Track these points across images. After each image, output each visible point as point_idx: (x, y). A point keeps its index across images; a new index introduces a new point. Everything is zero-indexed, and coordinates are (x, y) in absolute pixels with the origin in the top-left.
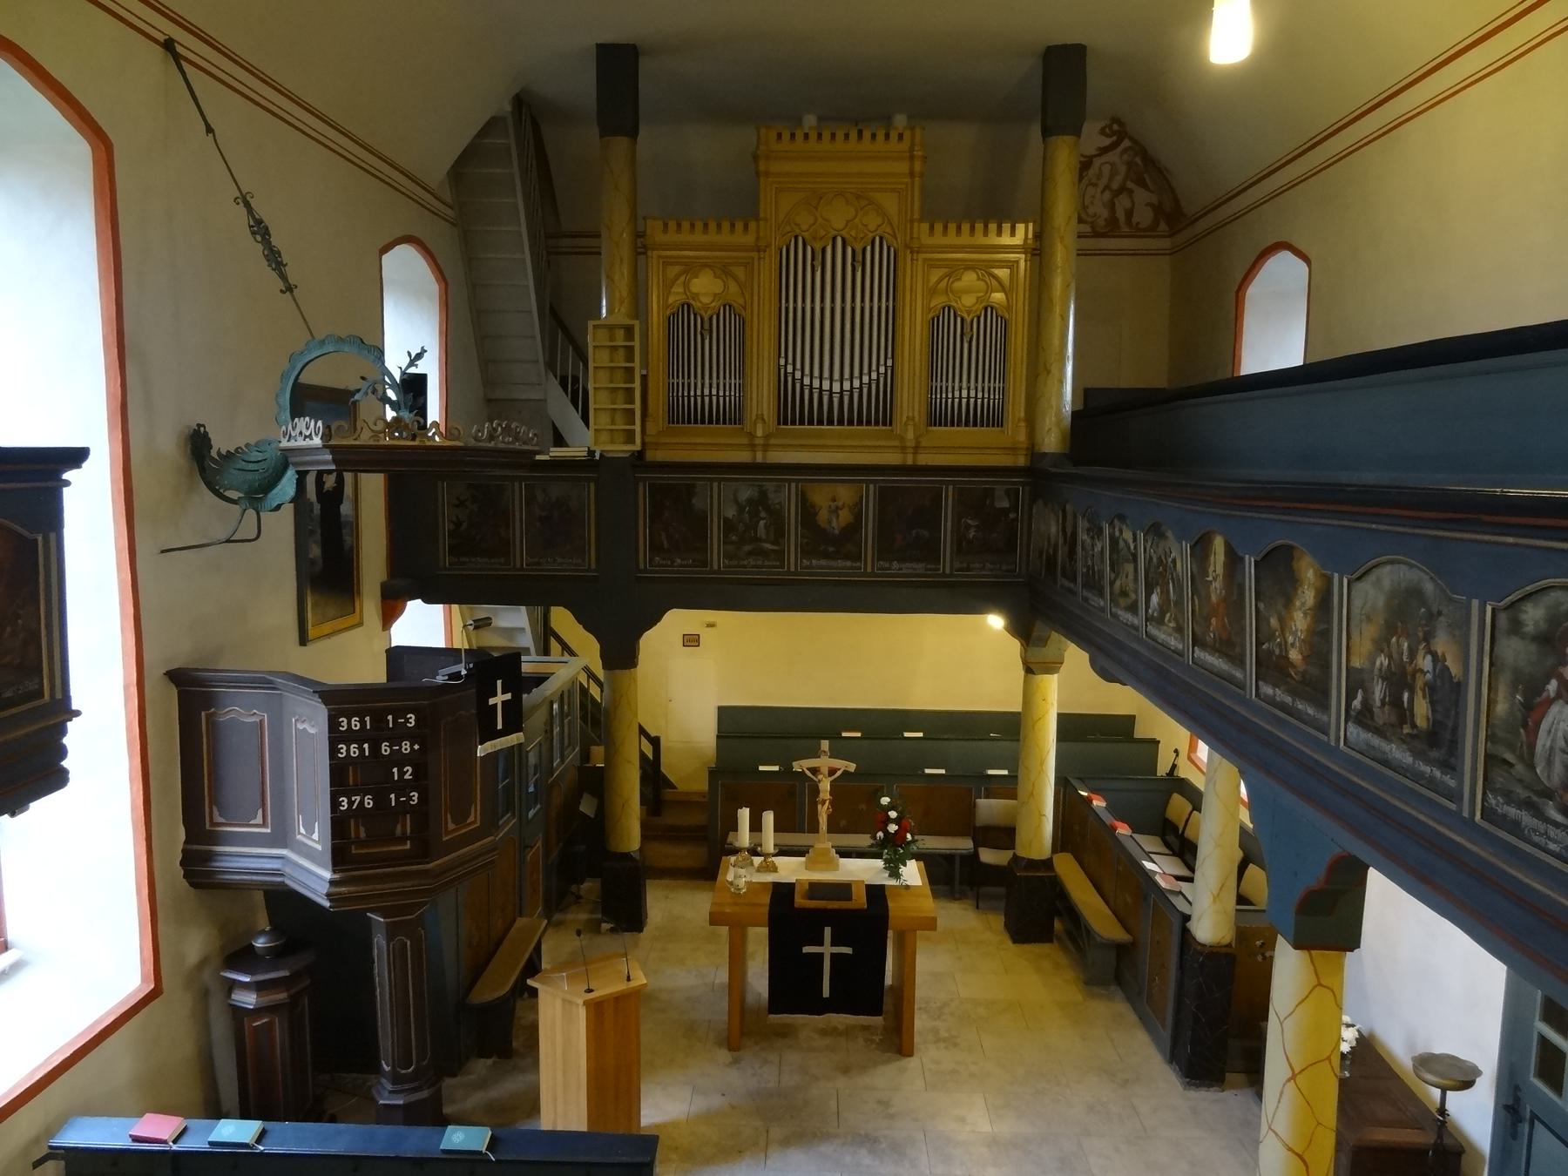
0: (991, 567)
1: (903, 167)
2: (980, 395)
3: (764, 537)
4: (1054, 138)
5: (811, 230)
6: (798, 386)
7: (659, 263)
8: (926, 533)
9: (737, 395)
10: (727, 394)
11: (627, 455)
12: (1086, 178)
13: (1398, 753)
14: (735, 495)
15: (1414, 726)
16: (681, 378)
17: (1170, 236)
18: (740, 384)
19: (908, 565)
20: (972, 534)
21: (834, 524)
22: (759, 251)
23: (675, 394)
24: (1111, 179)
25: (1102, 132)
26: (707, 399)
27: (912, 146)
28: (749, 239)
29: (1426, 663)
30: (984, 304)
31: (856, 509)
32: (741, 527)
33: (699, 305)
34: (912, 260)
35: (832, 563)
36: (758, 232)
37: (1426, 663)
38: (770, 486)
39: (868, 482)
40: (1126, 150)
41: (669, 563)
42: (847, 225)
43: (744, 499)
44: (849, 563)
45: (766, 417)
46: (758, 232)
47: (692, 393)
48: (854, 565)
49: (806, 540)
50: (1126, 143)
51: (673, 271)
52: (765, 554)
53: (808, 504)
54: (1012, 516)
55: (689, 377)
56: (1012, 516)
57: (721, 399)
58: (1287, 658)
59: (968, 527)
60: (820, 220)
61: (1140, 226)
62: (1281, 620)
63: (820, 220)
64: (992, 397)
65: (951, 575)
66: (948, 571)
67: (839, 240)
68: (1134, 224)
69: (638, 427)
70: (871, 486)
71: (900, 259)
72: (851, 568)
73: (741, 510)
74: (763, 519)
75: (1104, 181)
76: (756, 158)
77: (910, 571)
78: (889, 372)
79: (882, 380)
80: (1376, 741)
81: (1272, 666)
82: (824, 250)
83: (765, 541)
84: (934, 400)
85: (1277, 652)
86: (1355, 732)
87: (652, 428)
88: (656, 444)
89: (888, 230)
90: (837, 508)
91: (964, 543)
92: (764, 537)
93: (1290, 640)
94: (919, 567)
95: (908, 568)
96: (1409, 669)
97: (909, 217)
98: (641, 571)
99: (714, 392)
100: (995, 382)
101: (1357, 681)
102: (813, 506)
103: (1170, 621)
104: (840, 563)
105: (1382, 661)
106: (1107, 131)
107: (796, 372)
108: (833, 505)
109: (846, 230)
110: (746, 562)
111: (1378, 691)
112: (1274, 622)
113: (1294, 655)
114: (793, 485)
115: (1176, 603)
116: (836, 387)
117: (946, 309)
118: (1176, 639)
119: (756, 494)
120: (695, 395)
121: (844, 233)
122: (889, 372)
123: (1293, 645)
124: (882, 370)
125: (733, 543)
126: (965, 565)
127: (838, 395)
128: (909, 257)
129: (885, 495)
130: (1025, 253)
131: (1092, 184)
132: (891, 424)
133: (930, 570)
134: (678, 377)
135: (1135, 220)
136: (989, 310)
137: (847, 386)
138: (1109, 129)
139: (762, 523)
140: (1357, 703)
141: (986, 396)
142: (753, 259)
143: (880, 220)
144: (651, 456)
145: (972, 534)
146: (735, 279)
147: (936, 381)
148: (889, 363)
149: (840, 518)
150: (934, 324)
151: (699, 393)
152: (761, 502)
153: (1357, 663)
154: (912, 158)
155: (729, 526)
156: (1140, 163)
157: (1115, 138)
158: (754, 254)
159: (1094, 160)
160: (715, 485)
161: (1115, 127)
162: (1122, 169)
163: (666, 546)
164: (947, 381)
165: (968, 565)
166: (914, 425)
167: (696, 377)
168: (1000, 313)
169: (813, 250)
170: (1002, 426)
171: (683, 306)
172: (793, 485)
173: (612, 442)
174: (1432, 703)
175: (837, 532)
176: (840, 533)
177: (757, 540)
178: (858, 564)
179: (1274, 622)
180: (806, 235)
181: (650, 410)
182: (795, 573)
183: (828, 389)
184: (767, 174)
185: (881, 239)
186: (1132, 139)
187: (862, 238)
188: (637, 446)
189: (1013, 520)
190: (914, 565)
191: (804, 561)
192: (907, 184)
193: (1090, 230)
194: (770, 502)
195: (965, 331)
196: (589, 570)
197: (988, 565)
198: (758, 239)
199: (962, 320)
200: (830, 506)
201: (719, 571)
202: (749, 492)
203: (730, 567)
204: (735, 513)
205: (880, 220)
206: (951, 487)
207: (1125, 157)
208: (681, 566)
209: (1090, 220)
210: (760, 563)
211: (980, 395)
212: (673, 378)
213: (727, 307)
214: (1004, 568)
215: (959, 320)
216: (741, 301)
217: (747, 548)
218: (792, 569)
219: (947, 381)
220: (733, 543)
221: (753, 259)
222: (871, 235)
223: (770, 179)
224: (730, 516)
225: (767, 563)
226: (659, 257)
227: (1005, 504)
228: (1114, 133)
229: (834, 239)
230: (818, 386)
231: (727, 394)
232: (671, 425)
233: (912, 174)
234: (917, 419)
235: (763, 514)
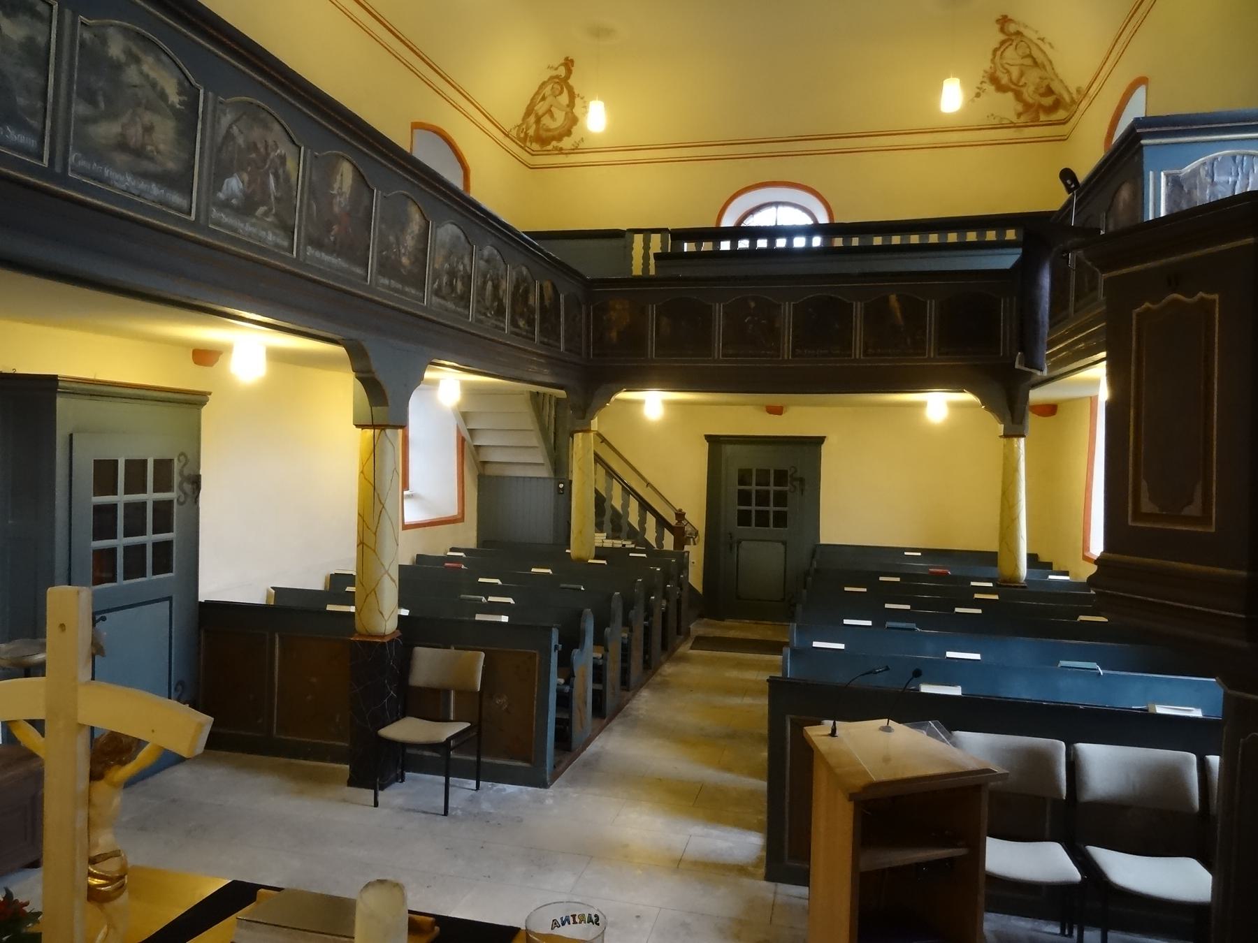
13: (450, 305)
15: (456, 292)
29: (461, 267)
37: (461, 267)
58: (400, 262)
62: (397, 239)
80: (443, 302)
81: (388, 267)
85: (393, 257)
86: (435, 300)
93: (403, 251)
96: (456, 270)
101: (437, 275)
103: (266, 214)
105: (447, 266)
111: (445, 279)
112: (392, 238)
113: (405, 260)
118: (274, 234)
123: (404, 254)
140: (435, 286)
153: (437, 266)
174: (463, 284)
179: (392, 238)
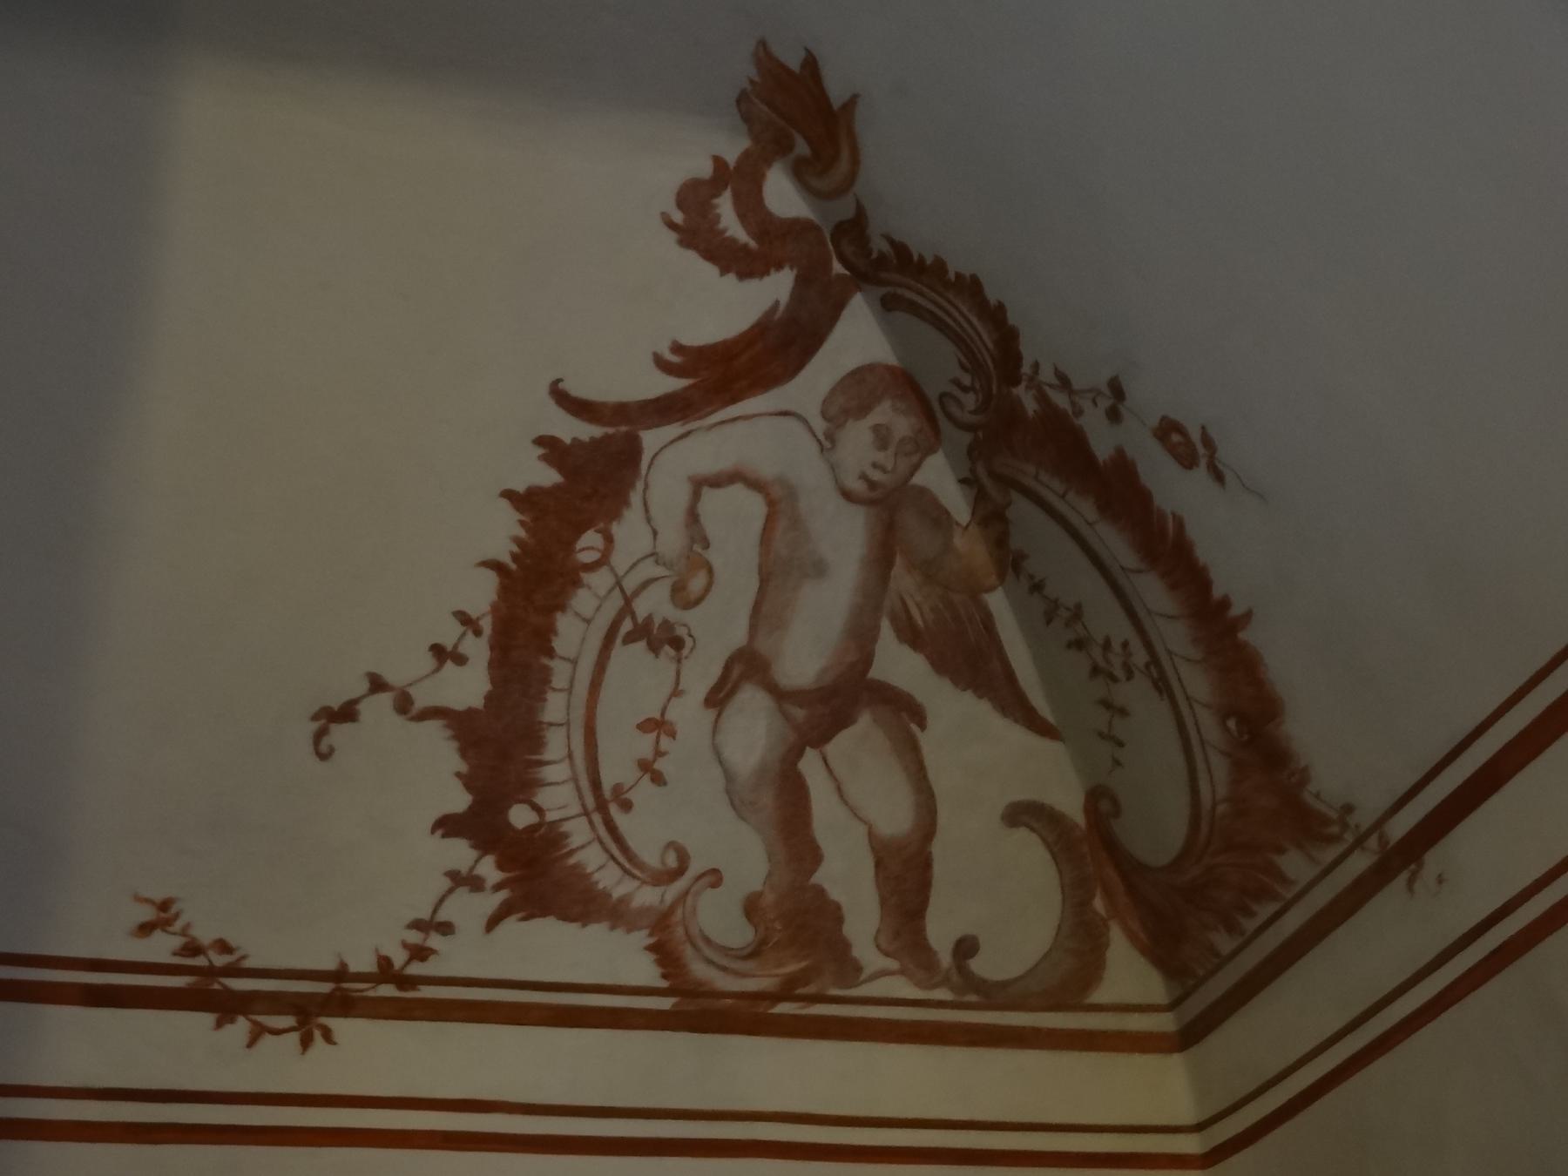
12: (599, 581)
17: (1187, 1038)
61: (978, 966)
68: (945, 959)
131: (642, 632)
135: (941, 932)
156: (957, 503)
157: (778, 287)
159: (651, 439)
193: (645, 971)
207: (857, 442)
209: (648, 897)
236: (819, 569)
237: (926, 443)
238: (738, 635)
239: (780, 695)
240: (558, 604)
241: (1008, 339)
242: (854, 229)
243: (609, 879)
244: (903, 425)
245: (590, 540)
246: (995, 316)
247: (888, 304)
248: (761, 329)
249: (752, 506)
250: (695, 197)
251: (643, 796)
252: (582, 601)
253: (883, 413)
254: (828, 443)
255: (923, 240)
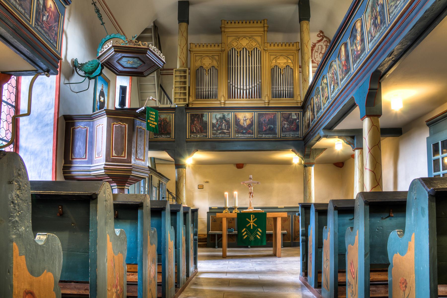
0: (293, 135)
1: (262, 29)
2: (286, 89)
3: (224, 128)
4: (303, 21)
5: (237, 46)
6: (234, 88)
7: (194, 55)
8: (272, 126)
9: (216, 91)
10: (213, 90)
11: (184, 106)
14: (216, 117)
16: (199, 86)
18: (217, 88)
19: (268, 136)
20: (286, 126)
21: (245, 124)
22: (222, 51)
23: (198, 91)
24: (321, 50)
25: (318, 36)
26: (207, 92)
27: (264, 24)
28: (219, 48)
30: (286, 65)
31: (252, 120)
32: (217, 126)
33: (205, 66)
34: (265, 53)
35: (245, 135)
36: (222, 46)
38: (226, 114)
39: (255, 112)
40: (325, 41)
41: (196, 136)
42: (246, 45)
43: (218, 117)
44: (250, 135)
45: (224, 96)
46: (222, 46)
47: (203, 90)
48: (251, 136)
49: (237, 129)
50: (325, 39)
51: (197, 58)
52: (224, 133)
53: (237, 119)
54: (297, 121)
55: (202, 86)
56: (297, 121)
57: (211, 92)
59: (285, 124)
60: (239, 43)
63: (239, 43)
64: (290, 90)
65: (280, 138)
66: (279, 137)
67: (245, 49)
69: (187, 97)
70: (256, 113)
71: (261, 53)
72: (250, 137)
73: (217, 121)
74: (224, 123)
75: (319, 51)
76: (221, 28)
77: (268, 137)
78: (260, 83)
79: (258, 86)
82: (240, 51)
83: (225, 130)
84: (273, 91)
87: (191, 99)
88: (193, 103)
89: (258, 46)
90: (246, 119)
91: (284, 129)
92: (224, 128)
94: (271, 136)
95: (267, 136)
97: (264, 42)
98: (188, 139)
99: (209, 90)
100: (291, 86)
102: (239, 119)
104: (247, 135)
106: (319, 35)
107: (233, 84)
108: (245, 119)
109: (246, 46)
110: (219, 136)
114: (233, 113)
115: (336, 79)
116: (245, 88)
117: (276, 66)
119: (222, 116)
120: (204, 91)
121: (246, 47)
122: (260, 83)
124: (258, 83)
125: (215, 130)
126: (284, 135)
127: (245, 90)
128: (264, 52)
129: (260, 115)
130: (297, 51)
131: (316, 52)
132: (261, 98)
133: (274, 137)
134: (199, 86)
136: (288, 66)
137: (248, 87)
138: (320, 35)
139: (224, 124)
141: (288, 89)
142: (220, 53)
143: (256, 44)
144: (190, 106)
145: (286, 126)
146: (215, 59)
147: (274, 86)
148: (260, 81)
149: (247, 122)
150: (272, 70)
151: (205, 90)
152: (224, 118)
154: (264, 27)
155: (213, 126)
157: (321, 38)
158: (221, 52)
159: (316, 44)
160: (210, 113)
161: (321, 34)
162: (324, 47)
163: (195, 131)
164: (277, 86)
165: (285, 135)
166: (268, 97)
167: (204, 86)
168: (291, 67)
169: (237, 51)
170: (293, 98)
171: (200, 67)
172: (233, 113)
173: (179, 102)
175: (246, 126)
176: (247, 126)
177: (222, 129)
178: (252, 136)
180: (235, 48)
181: (191, 94)
182: (234, 138)
183: (243, 88)
184: (224, 32)
185: (256, 48)
186: (326, 37)
187: (251, 48)
188: (187, 102)
189: (298, 122)
190: (269, 135)
191: (236, 135)
192: (263, 34)
194: (226, 118)
195: (281, 72)
196: (172, 139)
197: (291, 135)
198: (222, 48)
199: (280, 69)
200: (244, 119)
201: (211, 138)
202: (219, 116)
203: (214, 137)
204: (216, 122)
205: (256, 44)
206: (279, 113)
207: (325, 43)
208: (199, 137)
209: (317, 62)
210: (223, 136)
211: (286, 89)
212: (197, 86)
213: (213, 67)
214: (296, 136)
215: (279, 69)
216: (217, 65)
217: (219, 132)
218: (233, 137)
219: (277, 86)
220: (215, 130)
221: (220, 53)
222: (254, 47)
223: (225, 33)
224: (214, 122)
225: (225, 136)
226: (194, 54)
227: (295, 117)
228: (321, 36)
229: (243, 49)
230: (240, 88)
231: (213, 90)
232: (197, 99)
233: (264, 31)
234: (268, 95)
235: (224, 122)
236: (323, 48)
237: (328, 43)
238: (320, 51)
239: (322, 54)
240: (313, 51)
241: (330, 40)
242: (324, 36)
243: (315, 62)
244: (327, 42)
245: (314, 48)
246: (329, 39)
247: (326, 38)
248: (321, 39)
249: (320, 46)
250: (318, 35)
251: (317, 58)
252: (314, 51)
253: (326, 42)
254: (324, 43)
255: (326, 36)
